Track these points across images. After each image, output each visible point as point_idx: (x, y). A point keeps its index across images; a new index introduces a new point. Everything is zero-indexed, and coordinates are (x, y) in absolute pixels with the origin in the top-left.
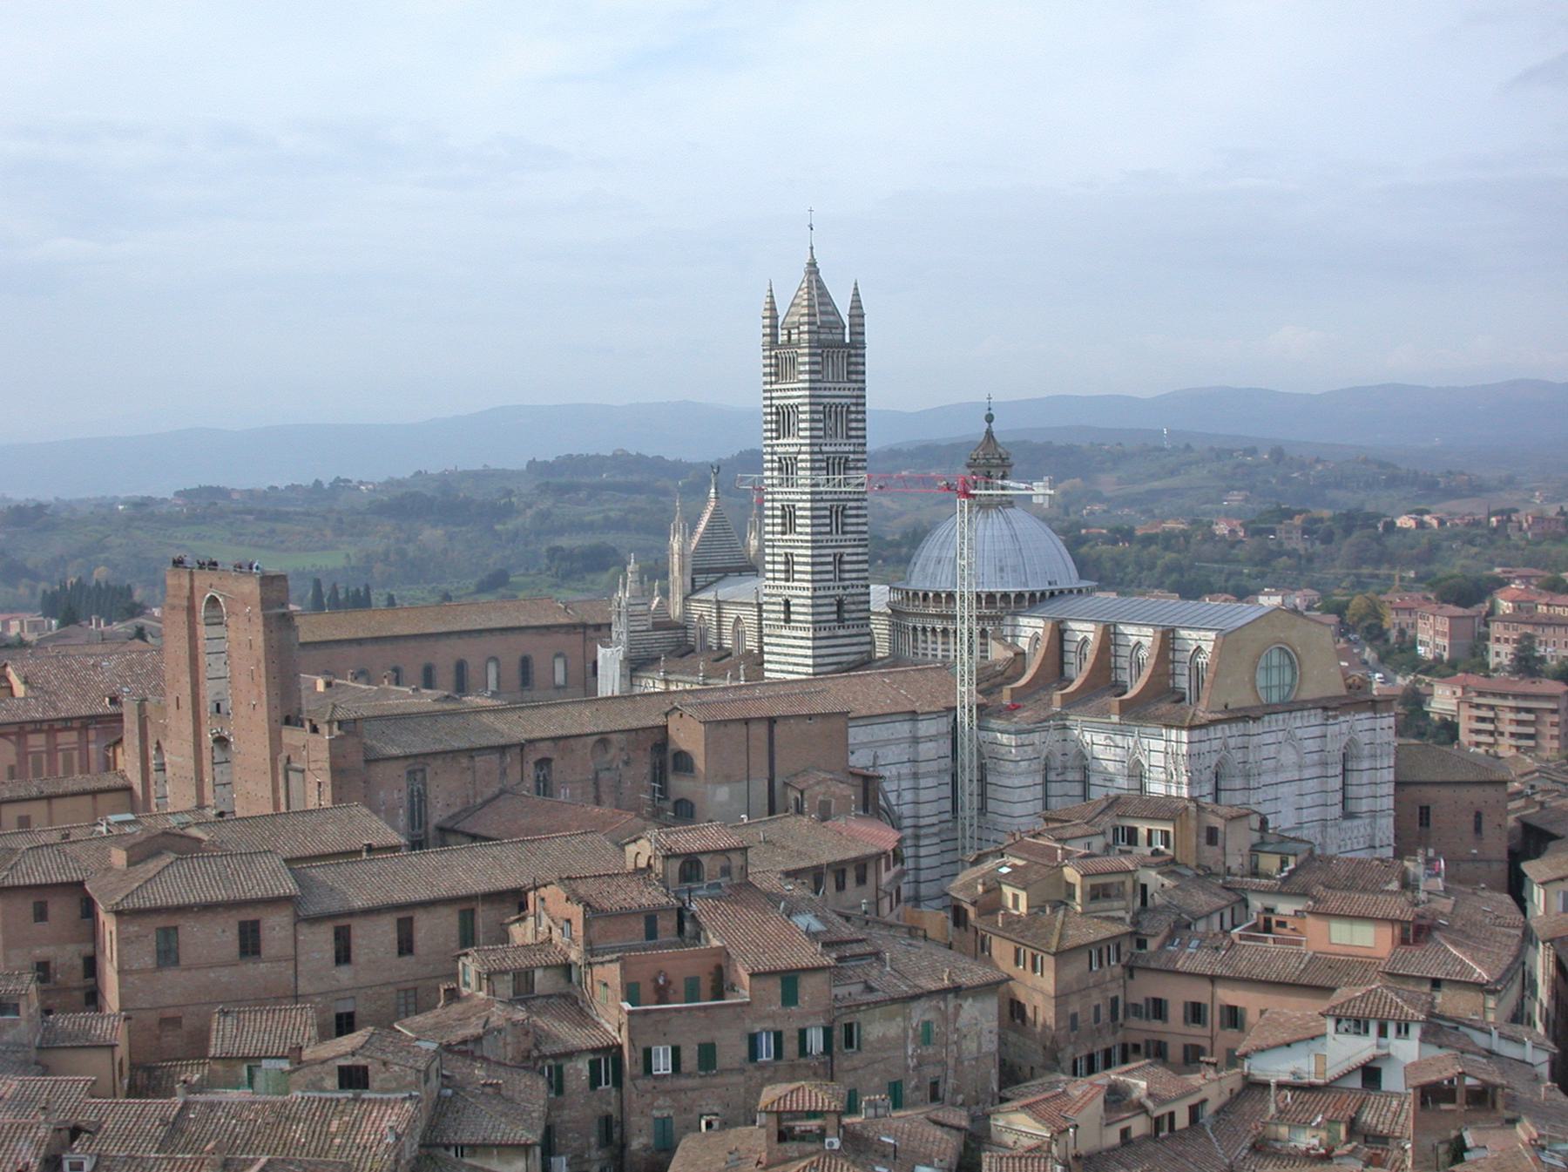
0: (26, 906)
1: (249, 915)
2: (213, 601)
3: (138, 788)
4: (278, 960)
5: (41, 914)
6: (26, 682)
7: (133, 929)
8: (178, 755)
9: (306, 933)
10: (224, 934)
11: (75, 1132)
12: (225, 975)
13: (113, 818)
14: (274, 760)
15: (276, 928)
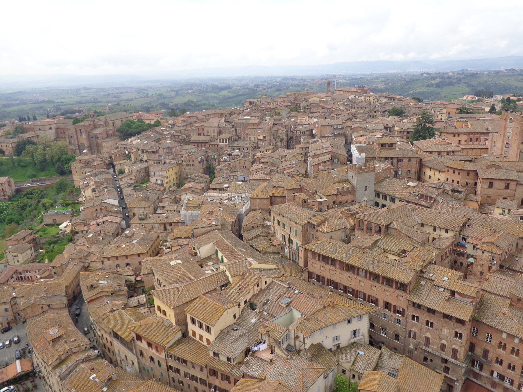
0: (466, 173)
1: (508, 182)
2: (511, 119)
3: (489, 149)
4: (512, 190)
5: (468, 174)
6: (471, 125)
7: (485, 181)
8: (499, 145)
9: (518, 187)
10: (503, 184)
11: (469, 219)
12: (501, 191)
13: (484, 155)
14: (518, 151)
15: (513, 185)
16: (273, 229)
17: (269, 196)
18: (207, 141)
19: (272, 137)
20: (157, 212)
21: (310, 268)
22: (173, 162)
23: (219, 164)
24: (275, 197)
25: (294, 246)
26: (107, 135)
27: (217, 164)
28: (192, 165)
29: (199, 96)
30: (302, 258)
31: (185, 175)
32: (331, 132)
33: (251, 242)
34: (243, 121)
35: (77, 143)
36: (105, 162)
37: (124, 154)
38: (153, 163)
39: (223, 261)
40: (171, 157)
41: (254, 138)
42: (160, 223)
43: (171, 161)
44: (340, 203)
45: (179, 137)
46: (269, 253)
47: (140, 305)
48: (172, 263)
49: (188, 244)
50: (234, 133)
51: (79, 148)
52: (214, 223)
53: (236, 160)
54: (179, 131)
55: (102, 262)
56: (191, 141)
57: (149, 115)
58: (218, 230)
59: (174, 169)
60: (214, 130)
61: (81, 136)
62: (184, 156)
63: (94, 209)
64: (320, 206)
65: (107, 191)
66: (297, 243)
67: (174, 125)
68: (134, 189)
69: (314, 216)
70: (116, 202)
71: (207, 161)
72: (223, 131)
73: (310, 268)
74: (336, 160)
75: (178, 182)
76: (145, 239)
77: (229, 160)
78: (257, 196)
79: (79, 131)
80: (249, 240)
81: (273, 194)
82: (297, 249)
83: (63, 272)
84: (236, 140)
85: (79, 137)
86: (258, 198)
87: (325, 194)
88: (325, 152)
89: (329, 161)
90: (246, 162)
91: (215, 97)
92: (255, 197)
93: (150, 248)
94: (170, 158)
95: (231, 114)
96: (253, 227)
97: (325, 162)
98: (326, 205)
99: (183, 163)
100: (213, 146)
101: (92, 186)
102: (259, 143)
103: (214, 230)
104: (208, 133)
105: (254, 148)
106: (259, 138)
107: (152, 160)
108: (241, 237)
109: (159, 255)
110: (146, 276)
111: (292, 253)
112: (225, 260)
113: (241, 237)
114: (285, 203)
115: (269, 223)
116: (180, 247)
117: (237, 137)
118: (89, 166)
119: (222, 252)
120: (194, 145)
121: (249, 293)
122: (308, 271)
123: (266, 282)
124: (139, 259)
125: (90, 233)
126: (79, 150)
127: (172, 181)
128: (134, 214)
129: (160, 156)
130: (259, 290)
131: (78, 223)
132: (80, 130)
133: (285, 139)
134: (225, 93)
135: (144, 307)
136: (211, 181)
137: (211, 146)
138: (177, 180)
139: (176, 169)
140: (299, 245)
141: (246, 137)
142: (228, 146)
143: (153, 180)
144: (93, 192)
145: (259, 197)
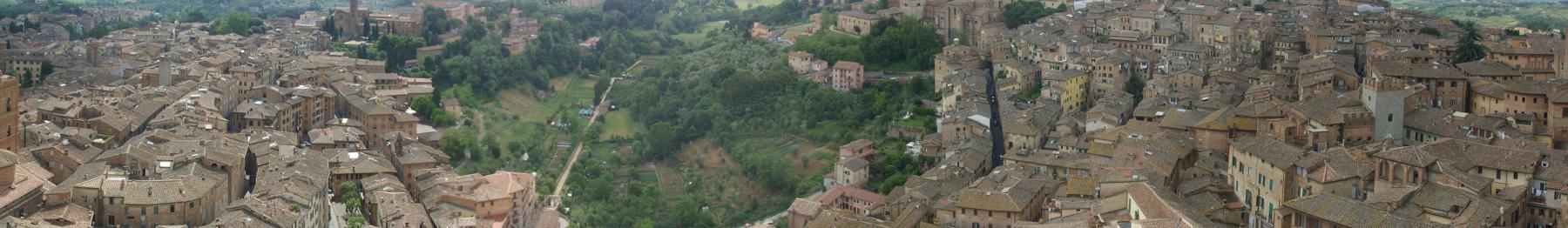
22: (1079, 67)
34: (1195, 12)
36: (980, 59)
38: (1048, 67)
40: (1077, 59)
55: (954, 213)
59: (1079, 78)
63: (954, 127)
68: (1015, 105)
70: (986, 121)
83: (899, 215)
99: (1094, 71)
101: (958, 91)
104: (1137, 26)
120: (1114, 44)
127: (1074, 97)
129: (1061, 58)
143: (1045, 93)
144: (957, 100)
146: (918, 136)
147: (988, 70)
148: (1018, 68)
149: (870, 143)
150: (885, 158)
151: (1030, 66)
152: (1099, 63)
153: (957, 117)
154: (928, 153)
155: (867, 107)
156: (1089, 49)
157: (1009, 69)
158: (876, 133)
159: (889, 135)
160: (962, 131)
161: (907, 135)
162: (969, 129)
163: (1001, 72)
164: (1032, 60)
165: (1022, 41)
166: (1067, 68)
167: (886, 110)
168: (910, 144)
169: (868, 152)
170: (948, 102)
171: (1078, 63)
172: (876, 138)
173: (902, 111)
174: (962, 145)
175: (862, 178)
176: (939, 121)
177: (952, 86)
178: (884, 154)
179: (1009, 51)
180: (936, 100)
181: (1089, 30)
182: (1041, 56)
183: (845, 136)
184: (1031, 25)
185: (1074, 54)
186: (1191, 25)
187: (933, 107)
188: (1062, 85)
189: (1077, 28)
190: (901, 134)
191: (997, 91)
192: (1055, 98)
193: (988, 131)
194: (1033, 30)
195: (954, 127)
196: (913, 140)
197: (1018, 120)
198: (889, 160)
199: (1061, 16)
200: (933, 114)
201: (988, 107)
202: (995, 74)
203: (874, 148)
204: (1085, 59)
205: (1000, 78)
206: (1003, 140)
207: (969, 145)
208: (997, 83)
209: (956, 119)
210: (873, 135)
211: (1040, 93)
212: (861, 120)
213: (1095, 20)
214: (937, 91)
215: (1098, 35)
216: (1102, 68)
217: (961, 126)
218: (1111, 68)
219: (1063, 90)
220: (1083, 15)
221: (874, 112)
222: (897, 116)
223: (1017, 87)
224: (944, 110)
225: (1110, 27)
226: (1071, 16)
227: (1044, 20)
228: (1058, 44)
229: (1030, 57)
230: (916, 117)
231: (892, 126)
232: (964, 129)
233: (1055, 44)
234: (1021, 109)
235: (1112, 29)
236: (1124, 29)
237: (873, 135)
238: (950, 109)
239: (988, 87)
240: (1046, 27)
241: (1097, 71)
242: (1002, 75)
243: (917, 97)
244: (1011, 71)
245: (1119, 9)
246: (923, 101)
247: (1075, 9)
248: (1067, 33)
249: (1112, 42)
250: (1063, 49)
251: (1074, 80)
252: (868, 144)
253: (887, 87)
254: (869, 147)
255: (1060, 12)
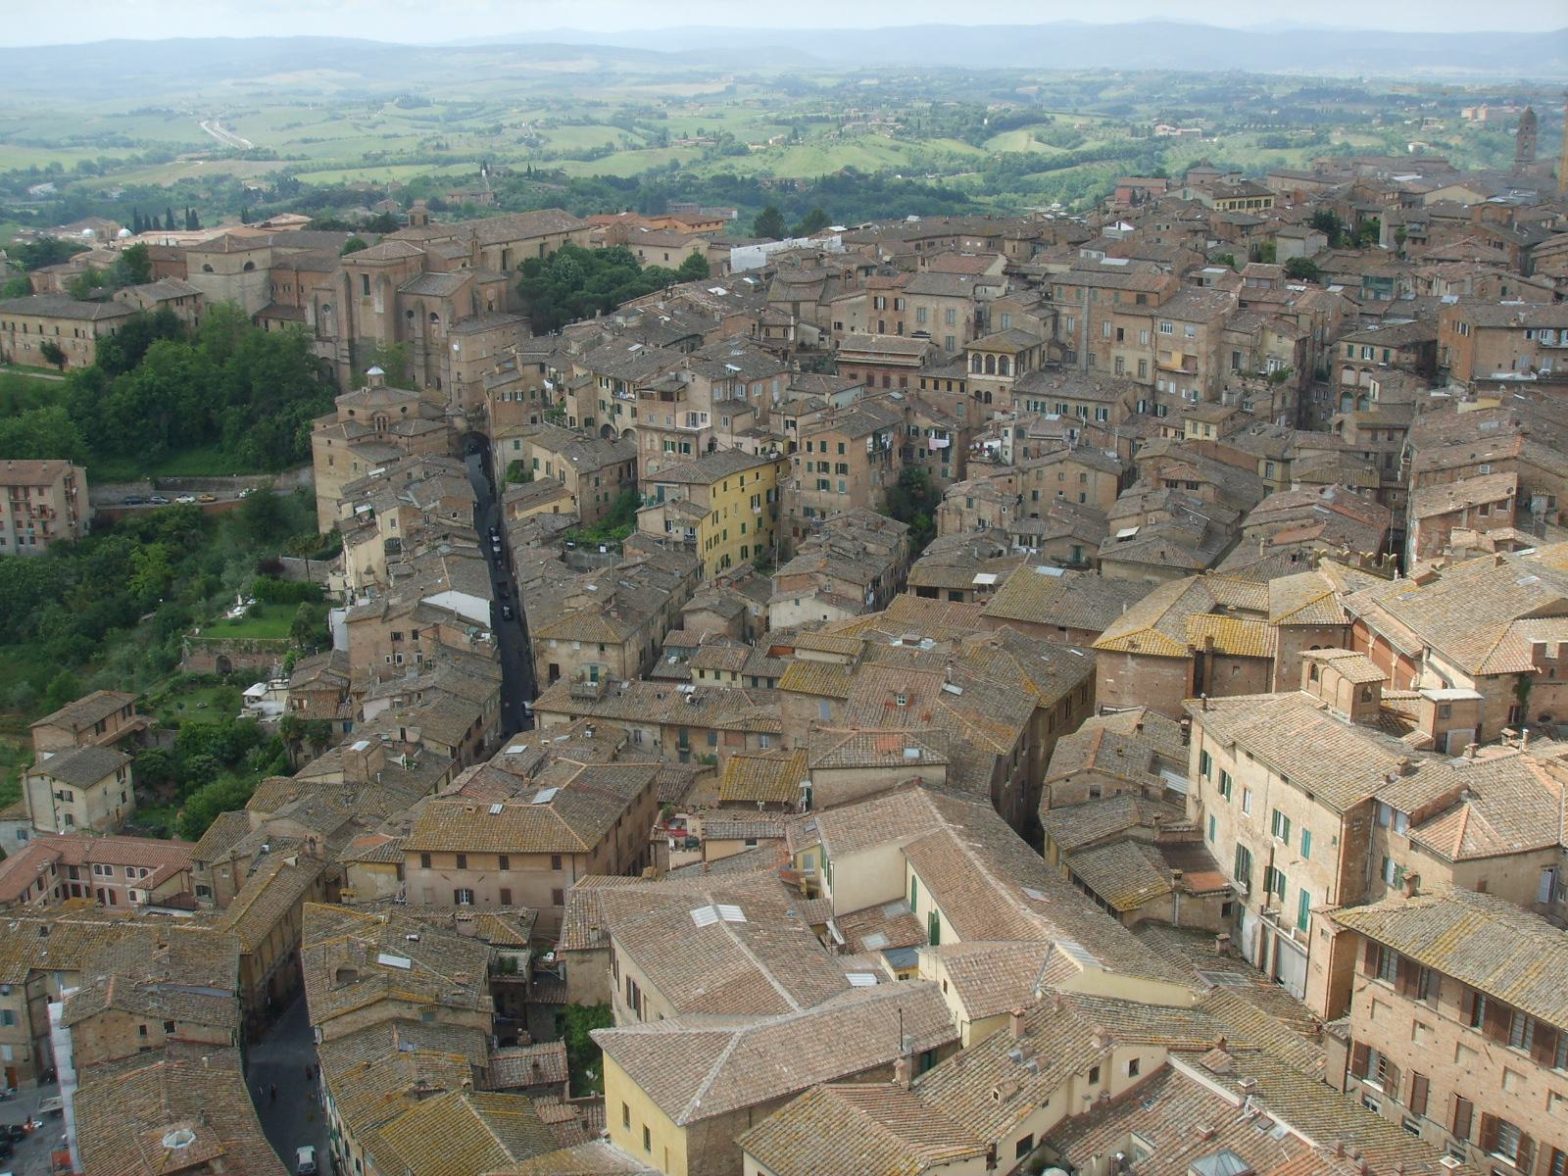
16: (1192, 812)
17: (1191, 648)
18: (916, 362)
19: (1228, 362)
20: (656, 673)
21: (1361, 1024)
22: (749, 445)
23: (962, 475)
24: (1218, 655)
25: (1289, 911)
26: (475, 306)
27: (952, 471)
28: (832, 469)
29: (896, 149)
30: (1325, 968)
31: (799, 513)
32: (1524, 362)
33: (1074, 864)
34: (1096, 279)
35: (345, 335)
36: (451, 427)
37: (538, 395)
39: (935, 939)
40: (744, 421)
41: (1142, 363)
42: (662, 726)
43: (741, 439)
44: (1544, 718)
45: (786, 333)
46: (1163, 925)
47: (539, 1088)
48: (702, 916)
49: (783, 839)
50: (1046, 332)
51: (351, 357)
52: (912, 753)
53: (1046, 460)
54: (788, 307)
55: (400, 867)
56: (843, 357)
57: (661, 224)
58: (928, 787)
59: (749, 477)
60: (950, 312)
61: (367, 303)
62: (800, 422)
63: (382, 632)
64: (1443, 726)
65: (446, 556)
66: (1305, 896)
67: (769, 275)
68: (563, 558)
69: (1408, 770)
70: (478, 608)
71: (906, 452)
72: (996, 321)
73: (1361, 1024)
74: (1539, 504)
75: (763, 540)
76: (589, 790)
77: (1009, 458)
78: (1133, 645)
79: (359, 283)
80: (1073, 853)
81: (1210, 640)
82: (1302, 923)
83: (237, 890)
84: (1052, 368)
85: (359, 309)
86: (1134, 655)
87: (1469, 669)
88: (1489, 455)
89: (1502, 504)
90: (1091, 476)
91: (973, 160)
92: (1122, 646)
93: (607, 836)
94: (738, 429)
95: (1035, 242)
96: (1095, 794)
97: (1484, 508)
98: (1472, 721)
99: (793, 458)
100: (943, 385)
101: (389, 525)
102: (1161, 386)
103: (909, 785)
105: (1133, 411)
106: (1164, 362)
107: (657, 430)
108: (1032, 833)
109: (646, 871)
110: (576, 957)
111: (1278, 938)
112: (948, 935)
113: (1032, 833)
114: (1267, 690)
115: (1173, 781)
116: (741, 846)
117: (1057, 353)
118: (385, 438)
119: (938, 893)
120: (853, 377)
121: (1046, 1104)
122: (1348, 1042)
123: (1133, 1068)
124: (558, 880)
125: (360, 736)
126: (353, 364)
127: (735, 533)
128: (554, 671)
129: (693, 419)
130: (1095, 1100)
131: (315, 686)
132: (366, 277)
133: (1293, 379)
134: (1019, 142)
135: (557, 1100)
136: (915, 554)
137: (930, 384)
138: (757, 532)
139: (756, 483)
140: (1313, 904)
141: (1099, 356)
142: (1012, 392)
143: (651, 521)
144: (388, 553)
145: (1142, 650)
146: (278, 665)
147: (479, 456)
148: (567, 451)
149: (128, 698)
150: (176, 736)
151: (602, 444)
152: (806, 431)
153: (392, 602)
154: (309, 710)
155: (112, 594)
156: (776, 390)
157: (541, 454)
158: (148, 667)
159: (187, 668)
160: (408, 640)
161: (241, 664)
162: (430, 634)
163: (518, 465)
164: (607, 427)
165: (578, 371)
166: (712, 446)
167: (168, 596)
168: (255, 690)
169: (125, 725)
170: (361, 558)
171: (746, 433)
172: (146, 681)
173: (220, 597)
174: (411, 679)
175: (115, 802)
176: (337, 618)
177: (372, 513)
178: (175, 726)
179: (539, 399)
180: (320, 557)
181: (776, 333)
182: (634, 413)
183: (50, 687)
184: (603, 321)
185: (732, 406)
186: (1083, 317)
187: (315, 578)
188: (699, 497)
189: (739, 330)
190: (223, 662)
191: (507, 519)
192: (678, 534)
193: (487, 636)
194: (608, 337)
195: (384, 631)
196: (264, 677)
197: (573, 603)
198: (193, 741)
199: (690, 292)
200: (317, 598)
201: (484, 567)
202: (499, 469)
203: (142, 711)
204: (766, 422)
205: (514, 480)
206: (531, 661)
207: (432, 678)
208: (506, 498)
209: (389, 608)
210: (139, 671)
211: (635, 520)
212: (96, 633)
213: (796, 304)
214: (325, 528)
215: (803, 347)
216: (816, 447)
217: (404, 626)
218: (841, 447)
219: (702, 512)
220: (758, 289)
221: (134, 604)
222: (209, 612)
223: (566, 505)
224: (352, 582)
225: (839, 326)
226: (722, 292)
227: (640, 306)
228: (686, 377)
229: (603, 418)
230: (266, 610)
231: (194, 644)
232: (415, 635)
233: (677, 379)
234: (582, 570)
235: (846, 330)
236: (882, 331)
237: (139, 671)
238: (369, 579)
239: (480, 510)
240: (649, 328)
241: (802, 457)
242: (520, 472)
243: (267, 552)
244: (547, 461)
245: (867, 269)
246: (284, 560)
247: (736, 268)
248: (712, 342)
249: (846, 371)
250: (701, 391)
251: (734, 482)
252: (120, 704)
253: (164, 528)
254: (126, 711)
255: (691, 278)
